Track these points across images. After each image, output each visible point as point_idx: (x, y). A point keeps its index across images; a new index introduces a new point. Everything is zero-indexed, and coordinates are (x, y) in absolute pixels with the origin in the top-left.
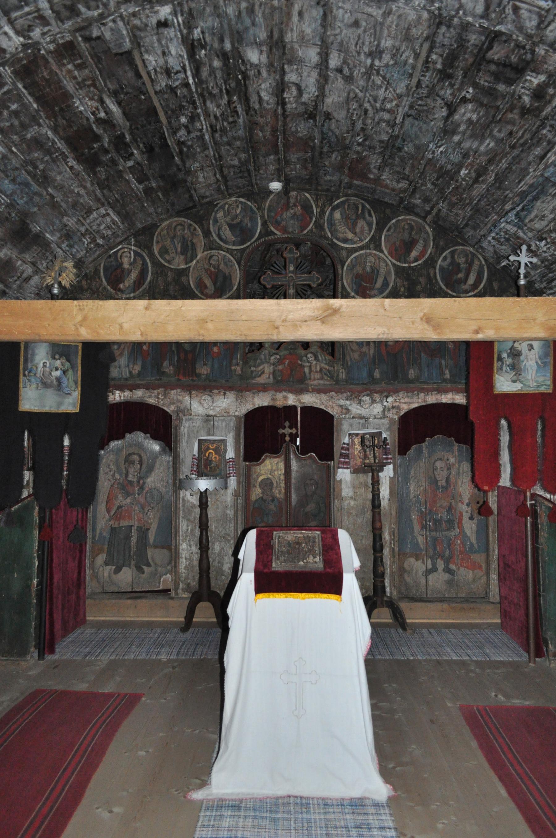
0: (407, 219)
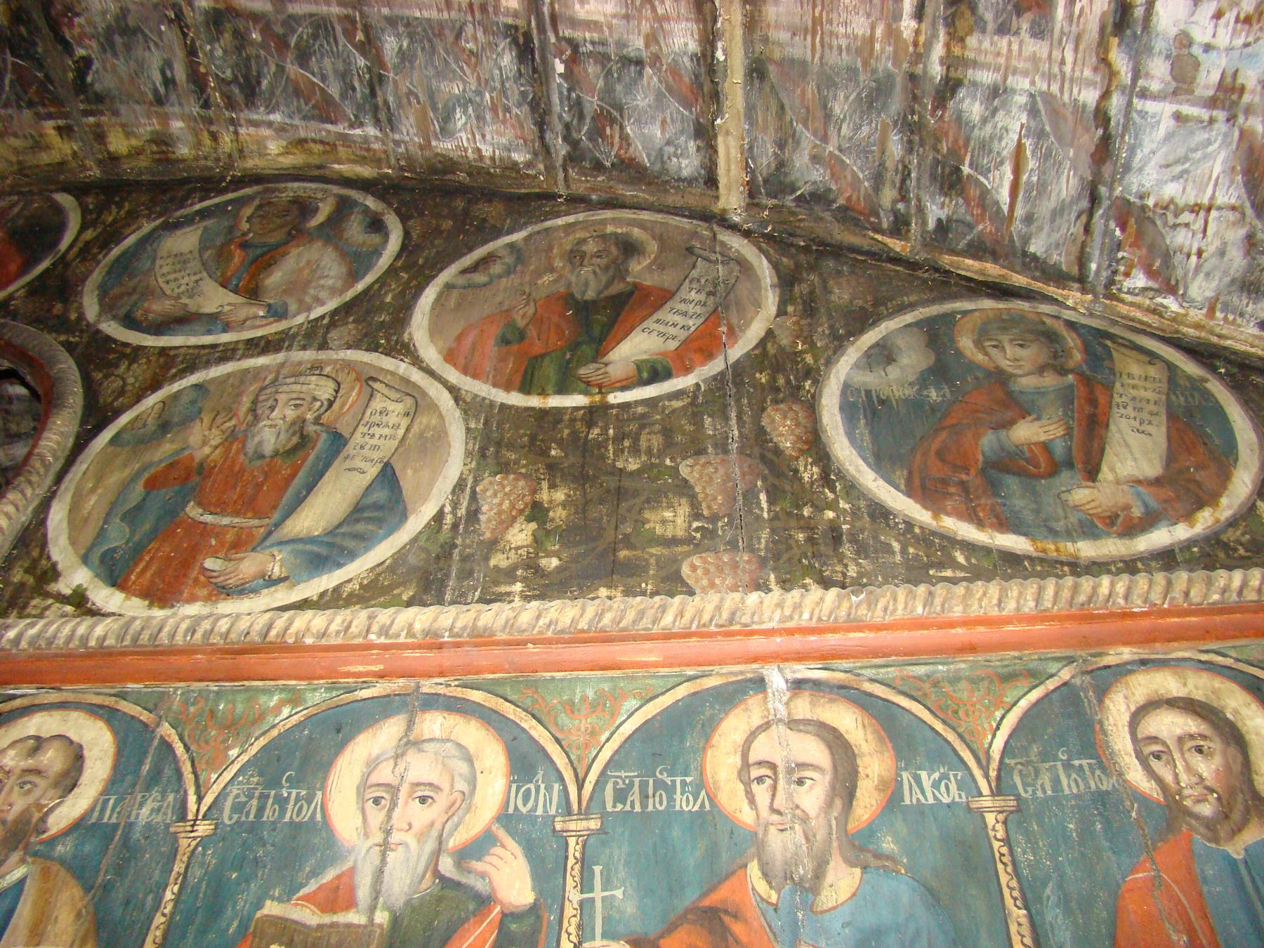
0: (604, 222)
